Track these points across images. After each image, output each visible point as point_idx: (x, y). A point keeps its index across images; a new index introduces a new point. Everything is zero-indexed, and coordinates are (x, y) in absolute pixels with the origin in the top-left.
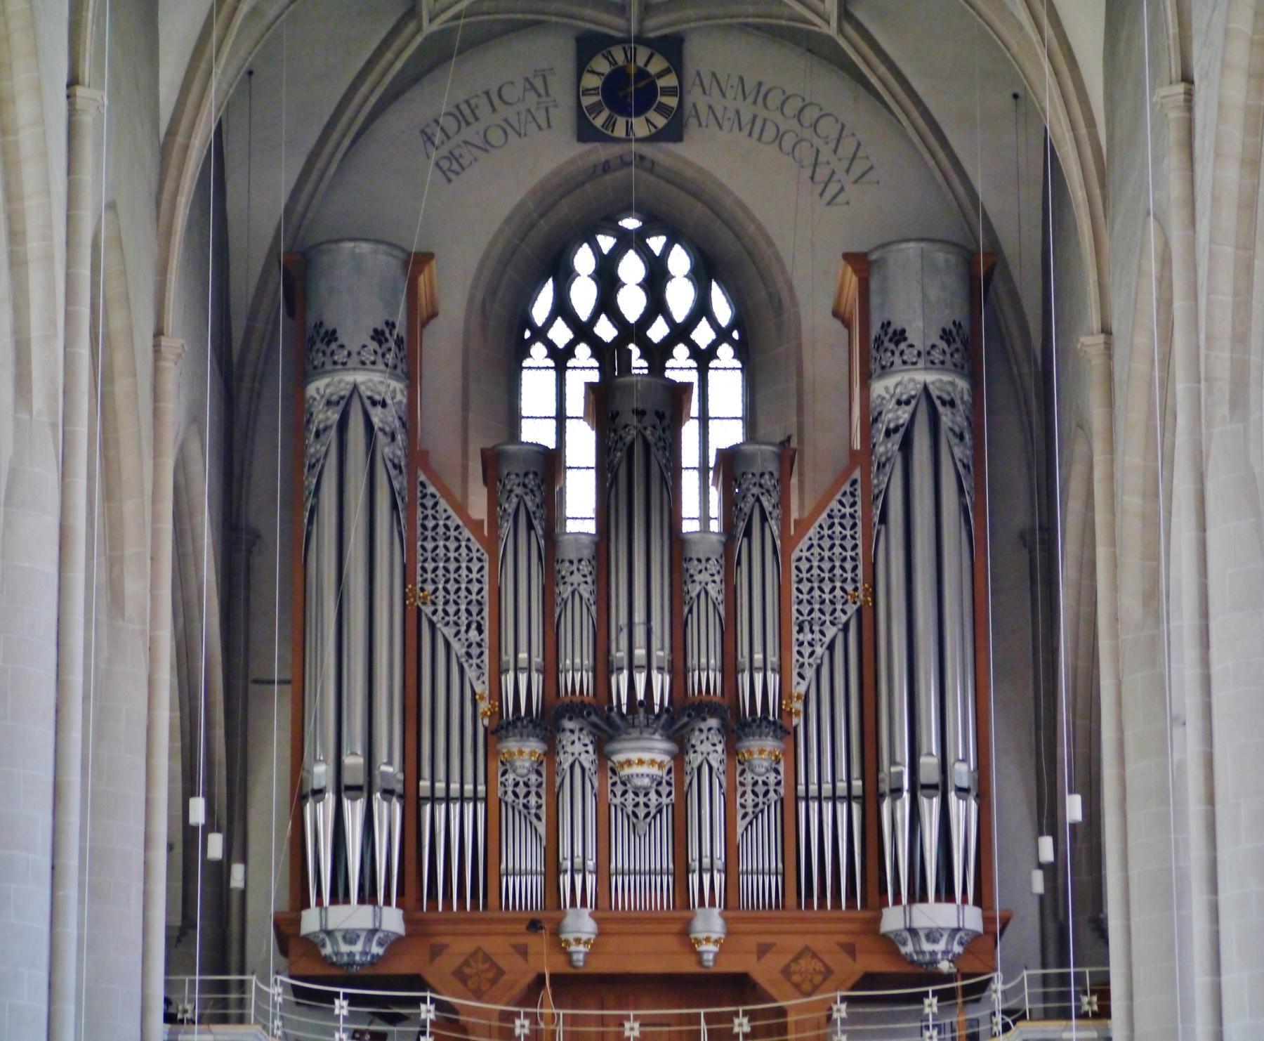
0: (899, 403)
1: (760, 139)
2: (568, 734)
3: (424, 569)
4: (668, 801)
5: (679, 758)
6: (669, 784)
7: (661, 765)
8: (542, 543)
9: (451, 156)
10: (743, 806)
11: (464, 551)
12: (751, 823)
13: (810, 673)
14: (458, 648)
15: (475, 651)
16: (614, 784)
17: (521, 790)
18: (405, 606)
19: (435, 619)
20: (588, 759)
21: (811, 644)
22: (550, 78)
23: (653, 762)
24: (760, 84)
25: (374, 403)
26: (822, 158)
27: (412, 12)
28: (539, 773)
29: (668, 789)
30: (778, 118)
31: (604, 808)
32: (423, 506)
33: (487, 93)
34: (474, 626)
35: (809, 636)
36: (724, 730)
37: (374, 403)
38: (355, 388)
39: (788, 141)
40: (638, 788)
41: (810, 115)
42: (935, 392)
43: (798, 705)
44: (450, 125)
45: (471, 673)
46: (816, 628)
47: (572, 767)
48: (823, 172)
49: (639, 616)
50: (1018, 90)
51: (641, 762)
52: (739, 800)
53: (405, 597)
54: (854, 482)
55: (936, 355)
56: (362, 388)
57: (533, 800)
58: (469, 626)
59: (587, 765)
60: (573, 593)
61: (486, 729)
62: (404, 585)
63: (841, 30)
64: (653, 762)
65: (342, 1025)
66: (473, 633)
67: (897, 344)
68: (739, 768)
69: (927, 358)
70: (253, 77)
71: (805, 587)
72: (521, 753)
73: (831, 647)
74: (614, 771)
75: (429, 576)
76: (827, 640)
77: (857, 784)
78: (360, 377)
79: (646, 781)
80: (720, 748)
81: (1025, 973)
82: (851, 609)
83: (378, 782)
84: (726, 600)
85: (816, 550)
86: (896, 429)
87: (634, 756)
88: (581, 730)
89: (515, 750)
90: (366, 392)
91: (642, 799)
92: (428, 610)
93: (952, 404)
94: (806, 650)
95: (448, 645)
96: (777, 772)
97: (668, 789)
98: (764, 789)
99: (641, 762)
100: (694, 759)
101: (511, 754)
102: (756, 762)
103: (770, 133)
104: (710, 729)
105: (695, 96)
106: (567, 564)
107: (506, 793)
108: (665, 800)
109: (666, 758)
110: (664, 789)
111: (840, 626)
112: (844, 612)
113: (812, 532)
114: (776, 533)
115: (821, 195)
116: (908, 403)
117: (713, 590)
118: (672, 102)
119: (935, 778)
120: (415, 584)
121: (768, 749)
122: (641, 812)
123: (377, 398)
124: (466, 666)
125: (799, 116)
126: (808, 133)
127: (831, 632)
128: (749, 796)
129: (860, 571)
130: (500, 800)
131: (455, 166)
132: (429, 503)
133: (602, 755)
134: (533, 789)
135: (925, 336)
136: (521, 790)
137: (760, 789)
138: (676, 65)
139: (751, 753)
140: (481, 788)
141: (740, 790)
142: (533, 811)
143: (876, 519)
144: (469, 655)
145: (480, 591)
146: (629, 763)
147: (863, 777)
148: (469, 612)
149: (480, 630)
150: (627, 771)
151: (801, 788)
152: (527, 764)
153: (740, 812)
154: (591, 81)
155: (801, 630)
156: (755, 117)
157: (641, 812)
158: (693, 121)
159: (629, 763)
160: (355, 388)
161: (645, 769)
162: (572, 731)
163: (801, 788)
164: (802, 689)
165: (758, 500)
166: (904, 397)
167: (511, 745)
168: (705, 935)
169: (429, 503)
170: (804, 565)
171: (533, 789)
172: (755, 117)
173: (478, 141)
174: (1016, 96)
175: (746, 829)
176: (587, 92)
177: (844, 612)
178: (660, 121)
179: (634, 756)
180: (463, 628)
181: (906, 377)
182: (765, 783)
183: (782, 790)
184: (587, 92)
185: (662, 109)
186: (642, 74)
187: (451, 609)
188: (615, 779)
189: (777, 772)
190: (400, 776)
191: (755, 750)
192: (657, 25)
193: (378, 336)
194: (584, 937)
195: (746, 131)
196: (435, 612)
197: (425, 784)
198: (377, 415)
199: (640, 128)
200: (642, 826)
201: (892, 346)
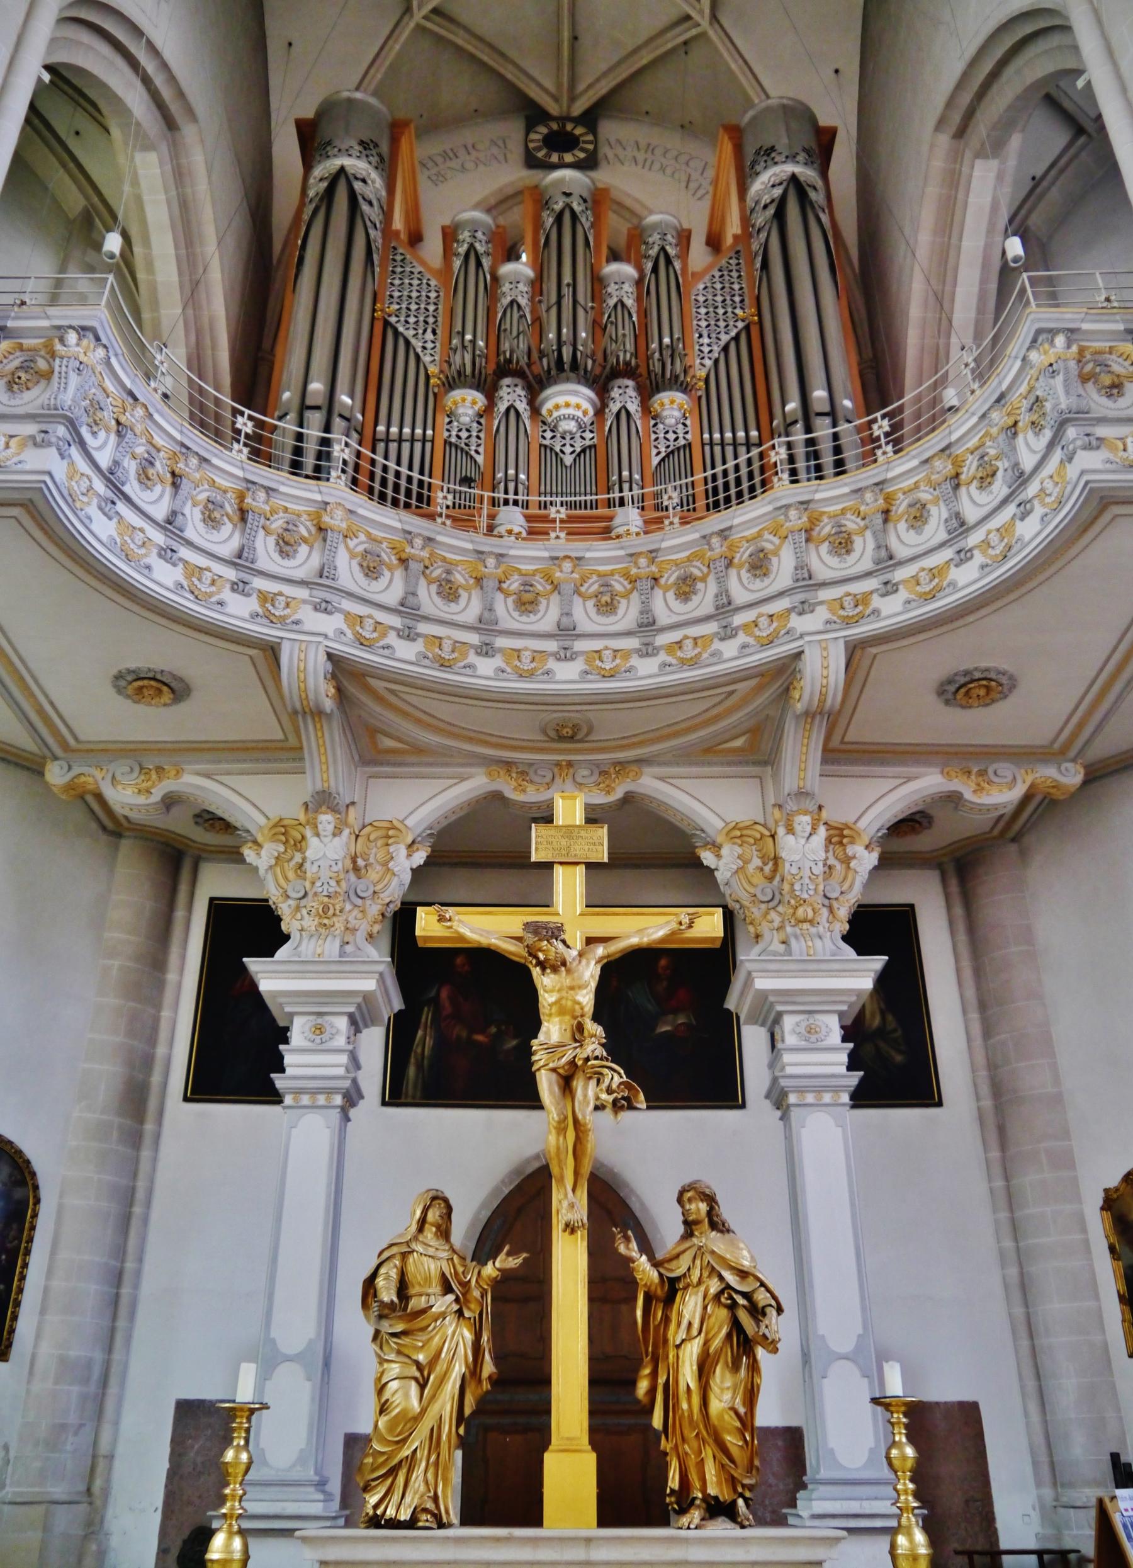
0: (773, 186)
1: (650, 169)
2: (505, 388)
3: (391, 296)
4: (591, 443)
5: (600, 412)
6: (592, 432)
7: (585, 413)
8: (488, 277)
9: (438, 174)
10: (656, 447)
11: (424, 286)
12: (663, 460)
13: (708, 363)
14: (417, 344)
15: (429, 345)
16: (544, 431)
17: (464, 434)
18: (373, 319)
19: (398, 325)
20: (522, 406)
21: (709, 345)
22: (507, 141)
23: (578, 407)
24: (649, 145)
25: (356, 178)
26: (693, 177)
27: (408, 10)
28: (479, 423)
29: (591, 435)
30: (663, 160)
31: (535, 447)
32: (394, 260)
33: (465, 147)
34: (429, 331)
35: (706, 340)
36: (639, 389)
37: (356, 178)
38: (342, 169)
39: (669, 171)
40: (565, 432)
41: (683, 159)
42: (802, 179)
43: (702, 384)
44: (439, 160)
45: (427, 359)
46: (713, 335)
47: (508, 410)
48: (692, 185)
49: (567, 279)
50: (836, 66)
51: (567, 405)
52: (653, 443)
53: (374, 310)
54: (738, 252)
55: (800, 158)
56: (347, 169)
57: (474, 440)
58: (425, 331)
59: (521, 410)
60: (512, 302)
61: (435, 395)
62: (374, 303)
63: (711, 24)
64: (578, 407)
65: (242, 439)
66: (429, 336)
67: (768, 155)
68: (652, 422)
69: (792, 158)
70: (293, 47)
71: (703, 311)
72: (464, 400)
73: (725, 349)
74: (544, 423)
75: (396, 300)
76: (722, 343)
77: (754, 433)
78: (347, 162)
79: (571, 426)
80: (637, 402)
81: (1025, 275)
82: (740, 325)
83: (337, 409)
84: (638, 312)
85: (710, 290)
86: (773, 201)
87: (561, 400)
88: (516, 385)
89: (458, 399)
90: (350, 171)
91: (568, 441)
92: (393, 319)
93: (815, 188)
94: (706, 349)
95: (407, 343)
96: (685, 425)
97: (591, 435)
98: (674, 436)
99: (567, 405)
100: (614, 407)
101: (455, 403)
102: (665, 413)
103: (657, 166)
104: (627, 387)
105: (604, 150)
106: (507, 285)
107: (450, 436)
108: (588, 443)
109: (591, 412)
110: (588, 435)
111: (733, 334)
112: (736, 327)
113: (707, 277)
114: (679, 272)
115: (694, 195)
116: (780, 184)
117: (630, 302)
118: (591, 147)
119: (826, 408)
120: (383, 304)
121: (678, 401)
122: (568, 449)
123: (359, 176)
124: (421, 354)
125: (676, 159)
126: (684, 167)
127: (725, 338)
128: (662, 441)
129: (747, 301)
130: (445, 441)
131: (441, 178)
132: (399, 258)
133: (535, 411)
134: (474, 434)
135: (790, 147)
136: (464, 434)
137: (671, 436)
138: (593, 129)
139: (662, 404)
140: (429, 432)
141: (653, 436)
142: (473, 448)
143: (758, 265)
144: (424, 348)
145: (436, 310)
146: (557, 407)
147: (758, 429)
148: (426, 322)
149: (434, 332)
150: (555, 414)
151: (706, 436)
152: (470, 412)
153: (654, 451)
154: (533, 136)
155: (701, 336)
156: (646, 160)
157: (568, 449)
158: (603, 164)
159: (557, 407)
160: (342, 169)
161: (570, 411)
162: (508, 386)
163: (706, 436)
164: (703, 373)
165: (663, 249)
166: (778, 181)
167: (457, 394)
168: (625, 528)
169: (399, 258)
170: (701, 299)
171: (474, 434)
172: (646, 160)
173: (458, 167)
174: (837, 71)
175: (659, 464)
176: (532, 141)
177: (736, 327)
178: (582, 155)
179: (561, 400)
180: (420, 331)
181: (777, 169)
182: (675, 432)
183: (689, 436)
184: (532, 141)
185: (583, 150)
186: (571, 134)
187: (412, 320)
188: (545, 427)
189: (685, 425)
190: (360, 417)
191: (666, 401)
192: (578, 109)
193: (362, 143)
194: (516, 529)
195: (640, 166)
196: (398, 321)
197: (381, 428)
198: (358, 186)
199: (568, 158)
200: (568, 460)
201: (765, 158)
